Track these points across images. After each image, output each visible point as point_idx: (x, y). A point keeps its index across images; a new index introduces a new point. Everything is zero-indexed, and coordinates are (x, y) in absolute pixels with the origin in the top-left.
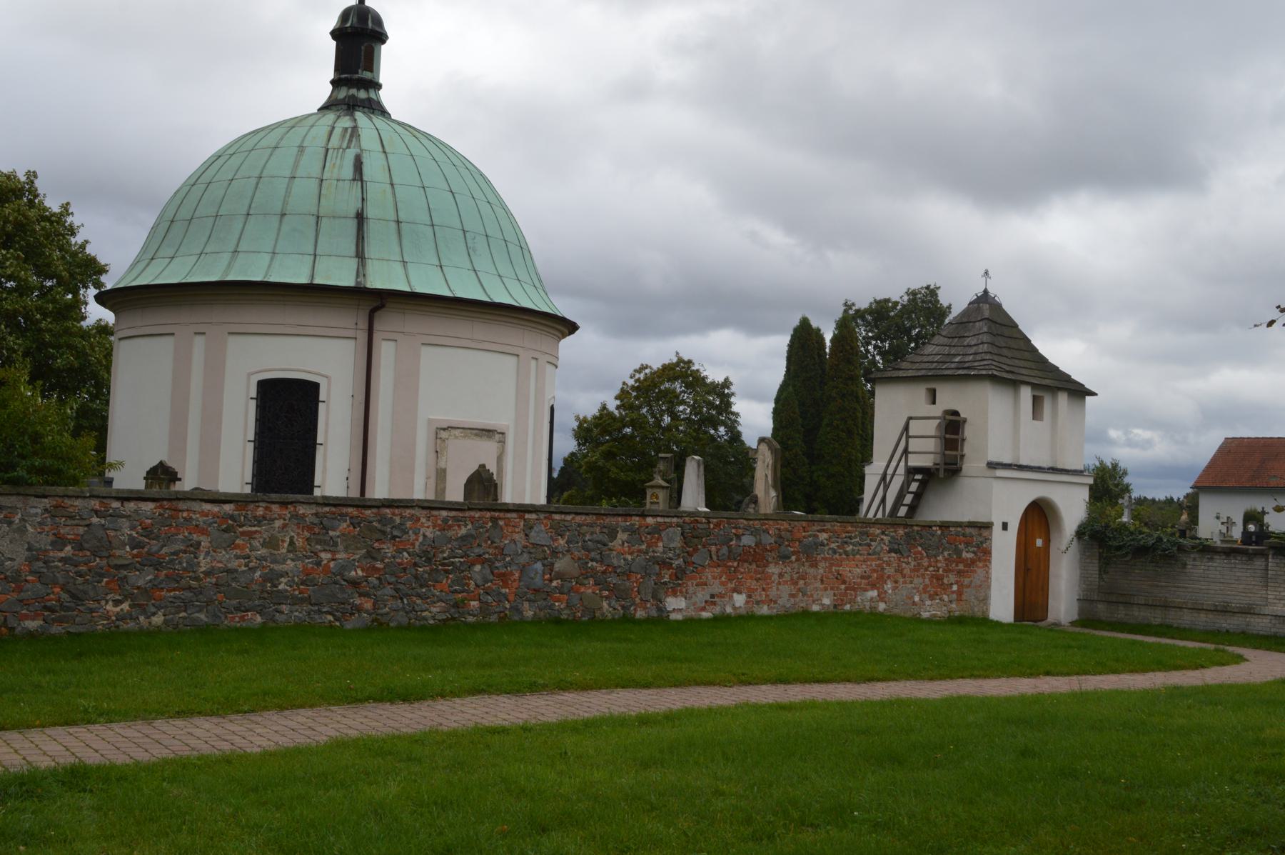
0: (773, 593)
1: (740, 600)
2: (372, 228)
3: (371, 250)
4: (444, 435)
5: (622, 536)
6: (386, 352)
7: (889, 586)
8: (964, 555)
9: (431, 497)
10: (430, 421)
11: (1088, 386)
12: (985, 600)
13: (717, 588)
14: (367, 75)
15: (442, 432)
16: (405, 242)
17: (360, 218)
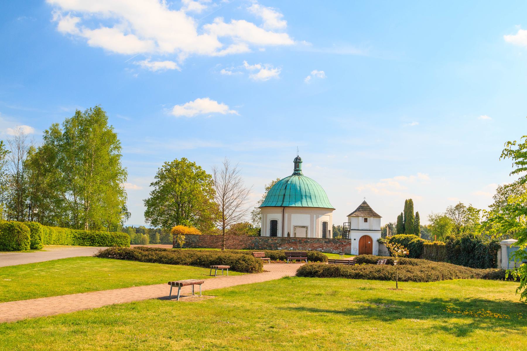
0: (298, 248)
1: (292, 249)
2: (286, 196)
3: (285, 200)
4: (295, 227)
5: (270, 240)
6: (286, 215)
7: (324, 248)
8: (344, 244)
9: (294, 237)
10: (293, 225)
11: (381, 216)
12: (350, 251)
13: (287, 247)
14: (298, 169)
15: (295, 227)
16: (290, 198)
17: (284, 195)
